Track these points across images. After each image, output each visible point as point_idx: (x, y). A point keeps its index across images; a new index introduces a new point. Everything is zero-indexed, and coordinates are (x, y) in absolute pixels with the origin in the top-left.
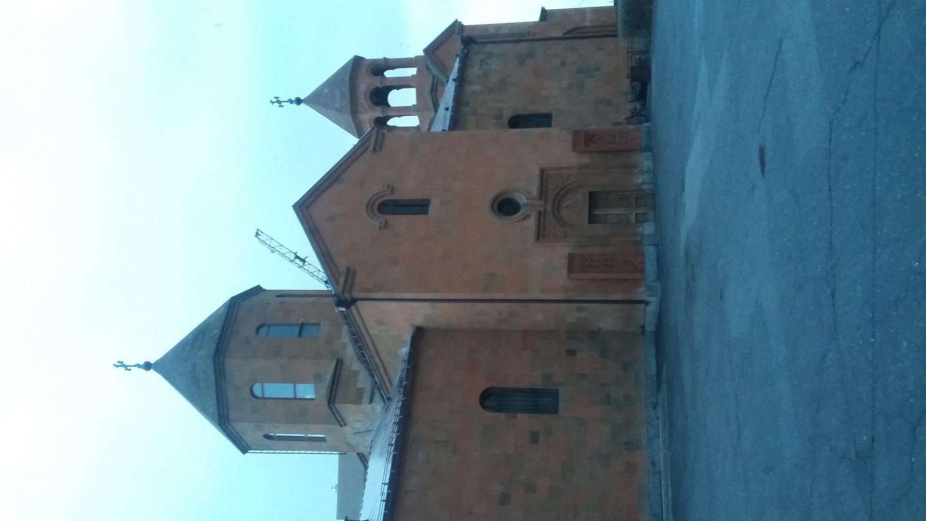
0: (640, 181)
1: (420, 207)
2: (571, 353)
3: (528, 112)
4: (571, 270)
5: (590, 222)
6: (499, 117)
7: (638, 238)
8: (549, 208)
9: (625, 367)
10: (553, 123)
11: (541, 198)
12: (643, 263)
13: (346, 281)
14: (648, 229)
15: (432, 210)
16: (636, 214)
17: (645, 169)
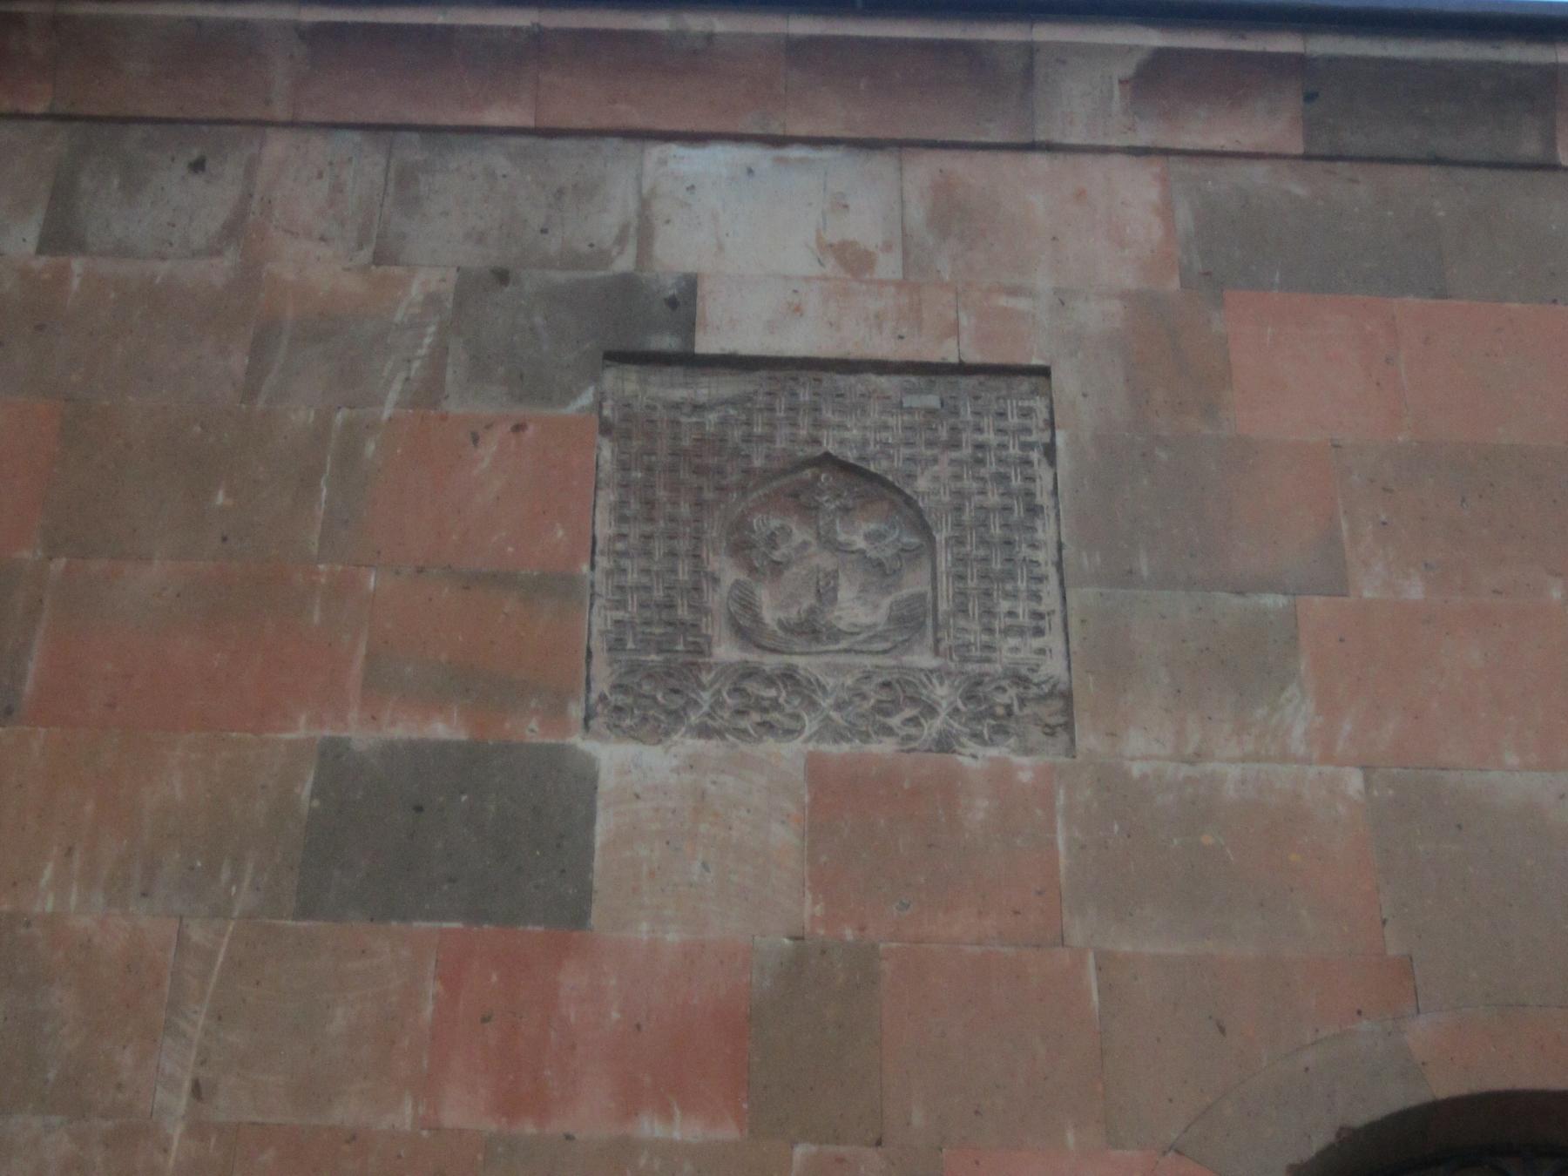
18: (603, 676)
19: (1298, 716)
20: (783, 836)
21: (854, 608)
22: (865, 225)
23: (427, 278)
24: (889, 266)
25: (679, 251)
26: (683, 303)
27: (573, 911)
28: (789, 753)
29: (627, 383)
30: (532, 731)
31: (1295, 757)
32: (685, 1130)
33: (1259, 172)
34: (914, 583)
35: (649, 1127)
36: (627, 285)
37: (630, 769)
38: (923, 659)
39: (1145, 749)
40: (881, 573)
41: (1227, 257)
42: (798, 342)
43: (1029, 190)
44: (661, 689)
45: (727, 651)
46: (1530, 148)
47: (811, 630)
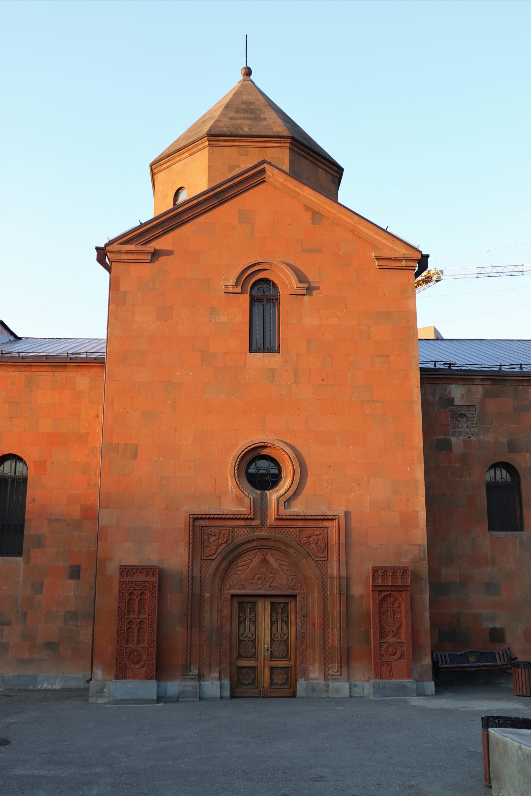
0: (311, 675)
1: (263, 338)
2: (75, 573)
3: (524, 493)
4: (125, 570)
5: (233, 596)
6: (512, 446)
7: (195, 671)
8: (264, 533)
9: (51, 646)
10: (502, 534)
11: (277, 519)
12: (136, 676)
13: (128, 252)
14: (213, 686)
15: (259, 359)
16: (255, 667)
17: (331, 684)
18: (451, 432)
19: (490, 435)
20: (462, 445)
21: (465, 426)
22: (463, 393)
23: (437, 398)
24: (465, 397)
25: (452, 395)
26: (453, 400)
27: (451, 451)
28: (461, 438)
29: (450, 407)
30: (448, 437)
31: (489, 438)
32: (458, 465)
33: (488, 386)
34: (468, 424)
35: (456, 465)
36: (449, 398)
37: (453, 439)
38: (468, 430)
39: (481, 437)
40: (466, 422)
41: (487, 394)
42: (460, 404)
43: (473, 388)
44: (454, 433)
45: (458, 430)
46: (506, 384)
47: (462, 427)
